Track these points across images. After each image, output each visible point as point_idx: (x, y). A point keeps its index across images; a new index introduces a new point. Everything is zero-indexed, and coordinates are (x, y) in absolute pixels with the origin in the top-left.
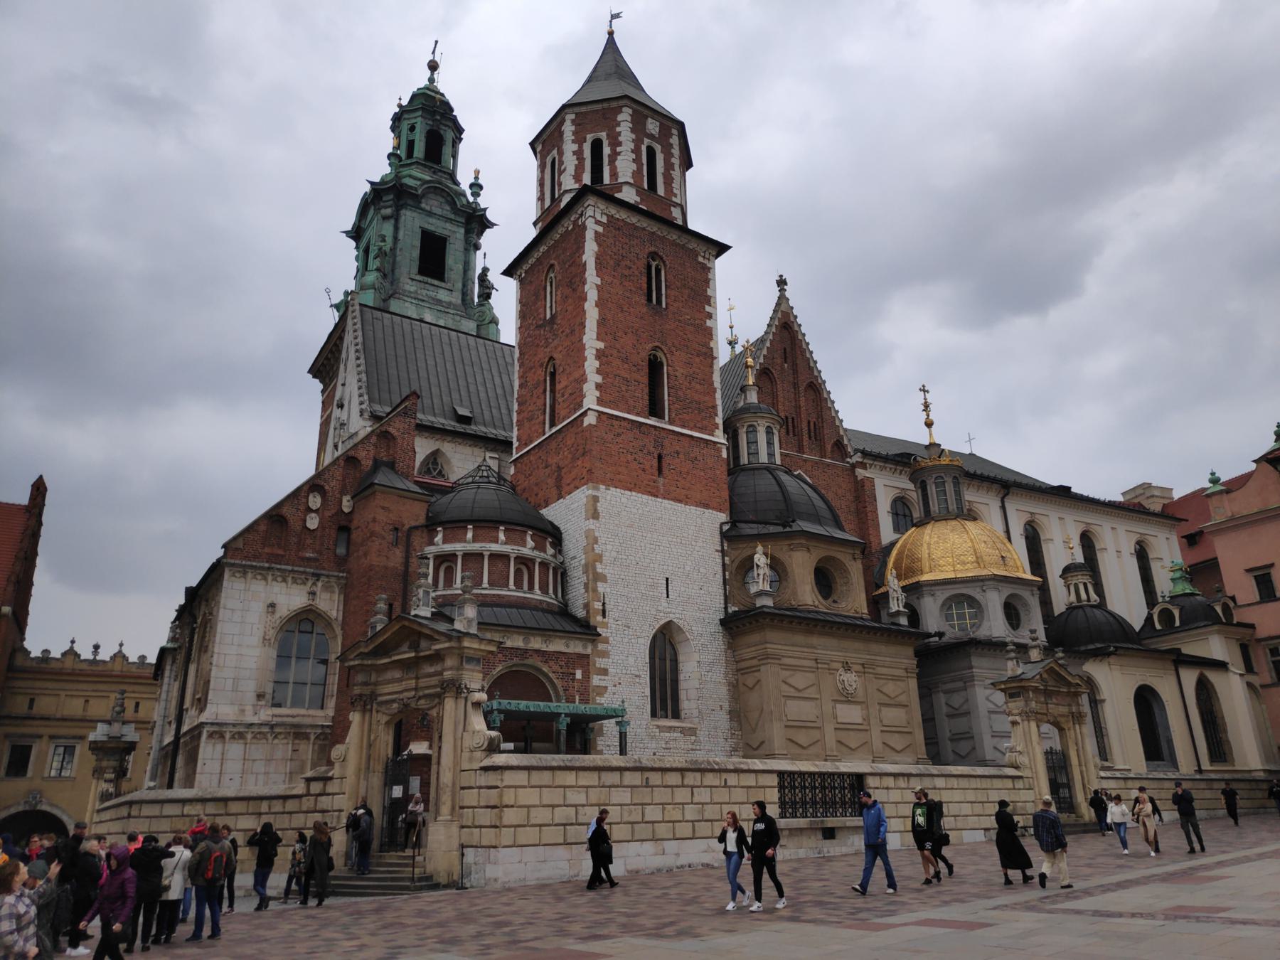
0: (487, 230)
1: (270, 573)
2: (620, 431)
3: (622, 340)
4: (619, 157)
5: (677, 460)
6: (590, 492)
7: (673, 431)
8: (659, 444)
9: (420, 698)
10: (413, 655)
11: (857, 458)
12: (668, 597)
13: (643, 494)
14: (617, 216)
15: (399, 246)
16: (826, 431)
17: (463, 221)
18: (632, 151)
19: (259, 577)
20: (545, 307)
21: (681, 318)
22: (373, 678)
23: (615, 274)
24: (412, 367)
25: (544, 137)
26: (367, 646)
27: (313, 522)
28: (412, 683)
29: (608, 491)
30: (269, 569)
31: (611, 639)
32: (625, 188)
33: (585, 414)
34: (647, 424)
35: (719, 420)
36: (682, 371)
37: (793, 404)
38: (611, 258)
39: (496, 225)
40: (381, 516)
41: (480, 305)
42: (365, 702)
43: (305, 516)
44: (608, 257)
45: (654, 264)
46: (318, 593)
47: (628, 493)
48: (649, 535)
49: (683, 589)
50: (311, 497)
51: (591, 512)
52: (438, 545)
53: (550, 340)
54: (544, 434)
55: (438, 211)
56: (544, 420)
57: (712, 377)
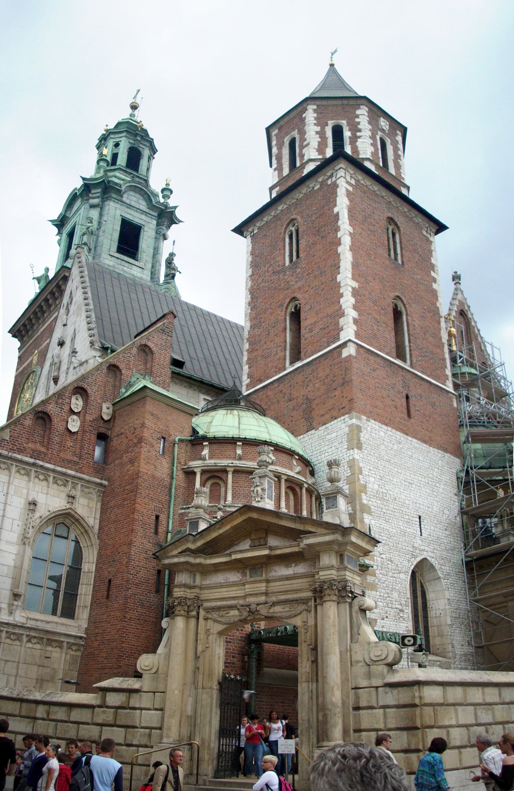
0: (174, 226)
1: (34, 469)
2: (376, 366)
3: (371, 284)
6: (354, 421)
7: (416, 375)
8: (406, 385)
9: (274, 604)
10: (266, 552)
12: (421, 535)
13: (396, 430)
15: (103, 228)
17: (156, 214)
19: (23, 472)
20: (284, 255)
21: (415, 277)
22: (198, 581)
24: (130, 314)
25: (282, 123)
26: (194, 541)
27: (74, 425)
28: (262, 587)
29: (370, 423)
30: (34, 465)
31: (378, 572)
33: (344, 345)
36: (417, 321)
38: (359, 212)
39: (182, 222)
40: (149, 422)
41: (166, 282)
42: (189, 607)
43: (68, 418)
46: (77, 497)
47: (384, 426)
48: (403, 472)
50: (73, 400)
51: (355, 442)
52: (204, 459)
53: (293, 283)
54: (285, 370)
55: (137, 206)
56: (285, 356)
57: (440, 333)
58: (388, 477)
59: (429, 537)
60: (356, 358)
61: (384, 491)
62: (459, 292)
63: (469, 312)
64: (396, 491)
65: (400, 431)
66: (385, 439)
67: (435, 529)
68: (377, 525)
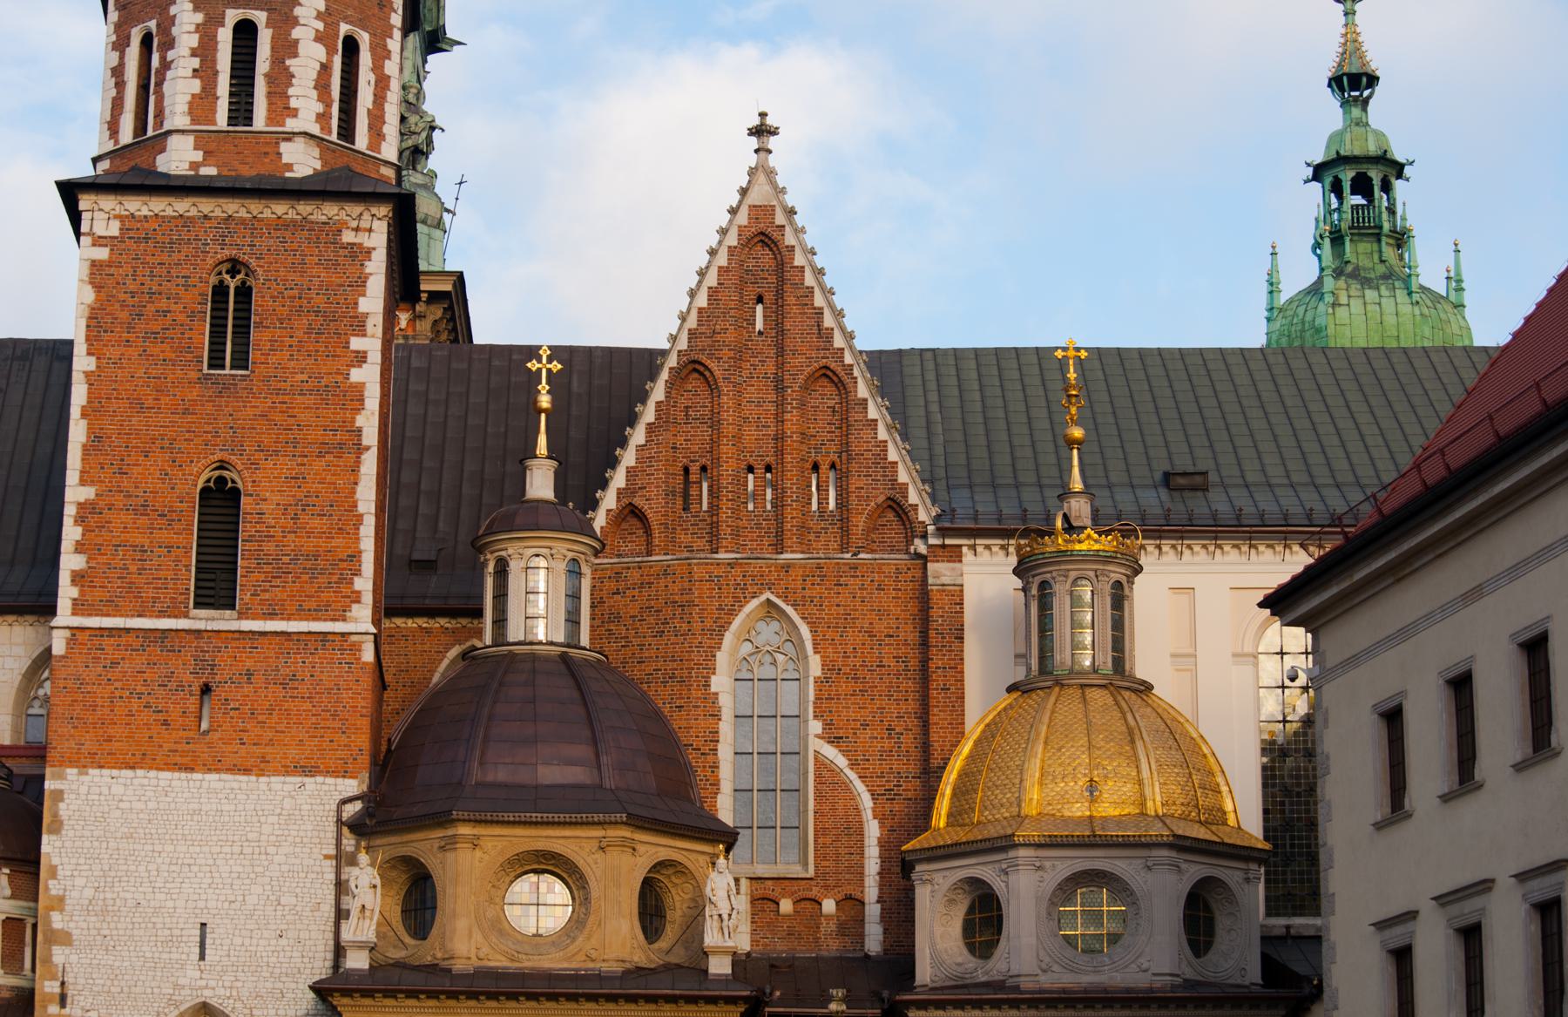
3: (136, 470)
4: (169, 74)
5: (247, 689)
11: (932, 541)
12: (202, 957)
13: (159, 769)
14: (145, 212)
16: (855, 482)
18: (194, 53)
23: (132, 337)
32: (174, 142)
34: (177, 630)
35: (364, 584)
36: (276, 498)
37: (771, 431)
38: (124, 305)
44: (117, 306)
45: (232, 284)
48: (170, 848)
49: (238, 941)
57: (355, 493)
58: (121, 868)
59: (226, 959)
60: (63, 657)
61: (109, 895)
62: (761, 178)
63: (788, 229)
64: (140, 889)
65: (169, 770)
66: (124, 798)
67: (247, 941)
68: (84, 961)
